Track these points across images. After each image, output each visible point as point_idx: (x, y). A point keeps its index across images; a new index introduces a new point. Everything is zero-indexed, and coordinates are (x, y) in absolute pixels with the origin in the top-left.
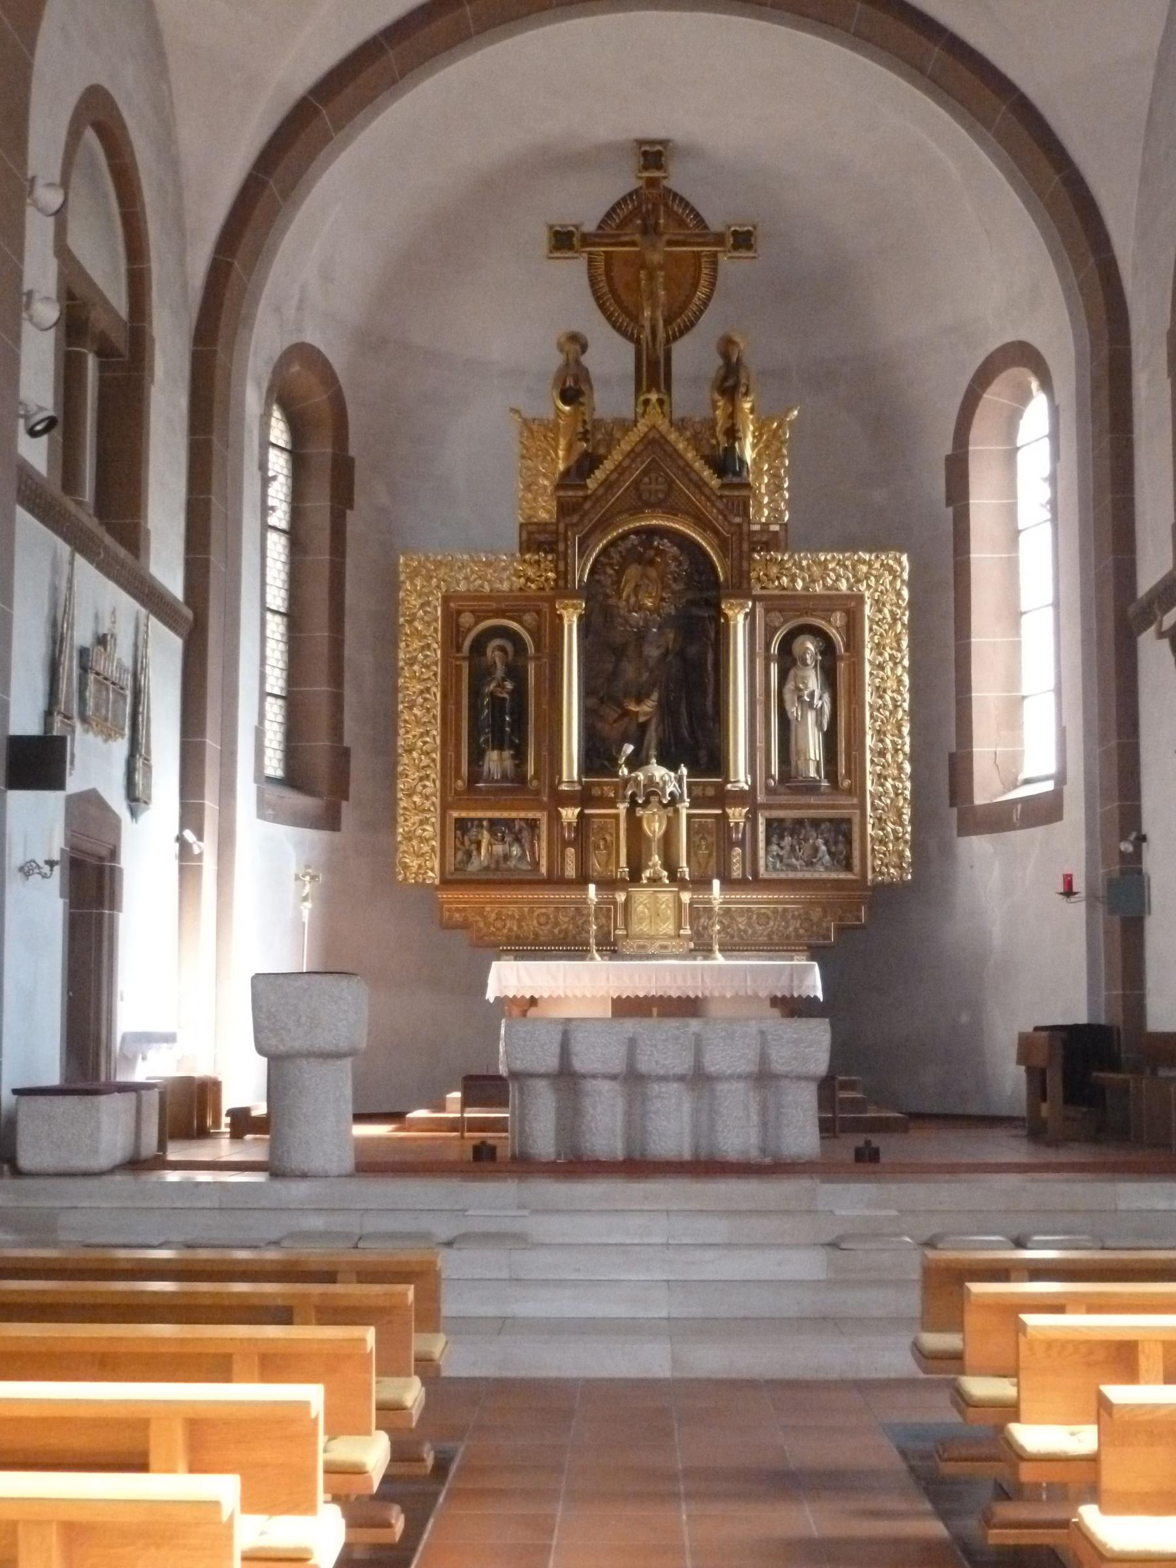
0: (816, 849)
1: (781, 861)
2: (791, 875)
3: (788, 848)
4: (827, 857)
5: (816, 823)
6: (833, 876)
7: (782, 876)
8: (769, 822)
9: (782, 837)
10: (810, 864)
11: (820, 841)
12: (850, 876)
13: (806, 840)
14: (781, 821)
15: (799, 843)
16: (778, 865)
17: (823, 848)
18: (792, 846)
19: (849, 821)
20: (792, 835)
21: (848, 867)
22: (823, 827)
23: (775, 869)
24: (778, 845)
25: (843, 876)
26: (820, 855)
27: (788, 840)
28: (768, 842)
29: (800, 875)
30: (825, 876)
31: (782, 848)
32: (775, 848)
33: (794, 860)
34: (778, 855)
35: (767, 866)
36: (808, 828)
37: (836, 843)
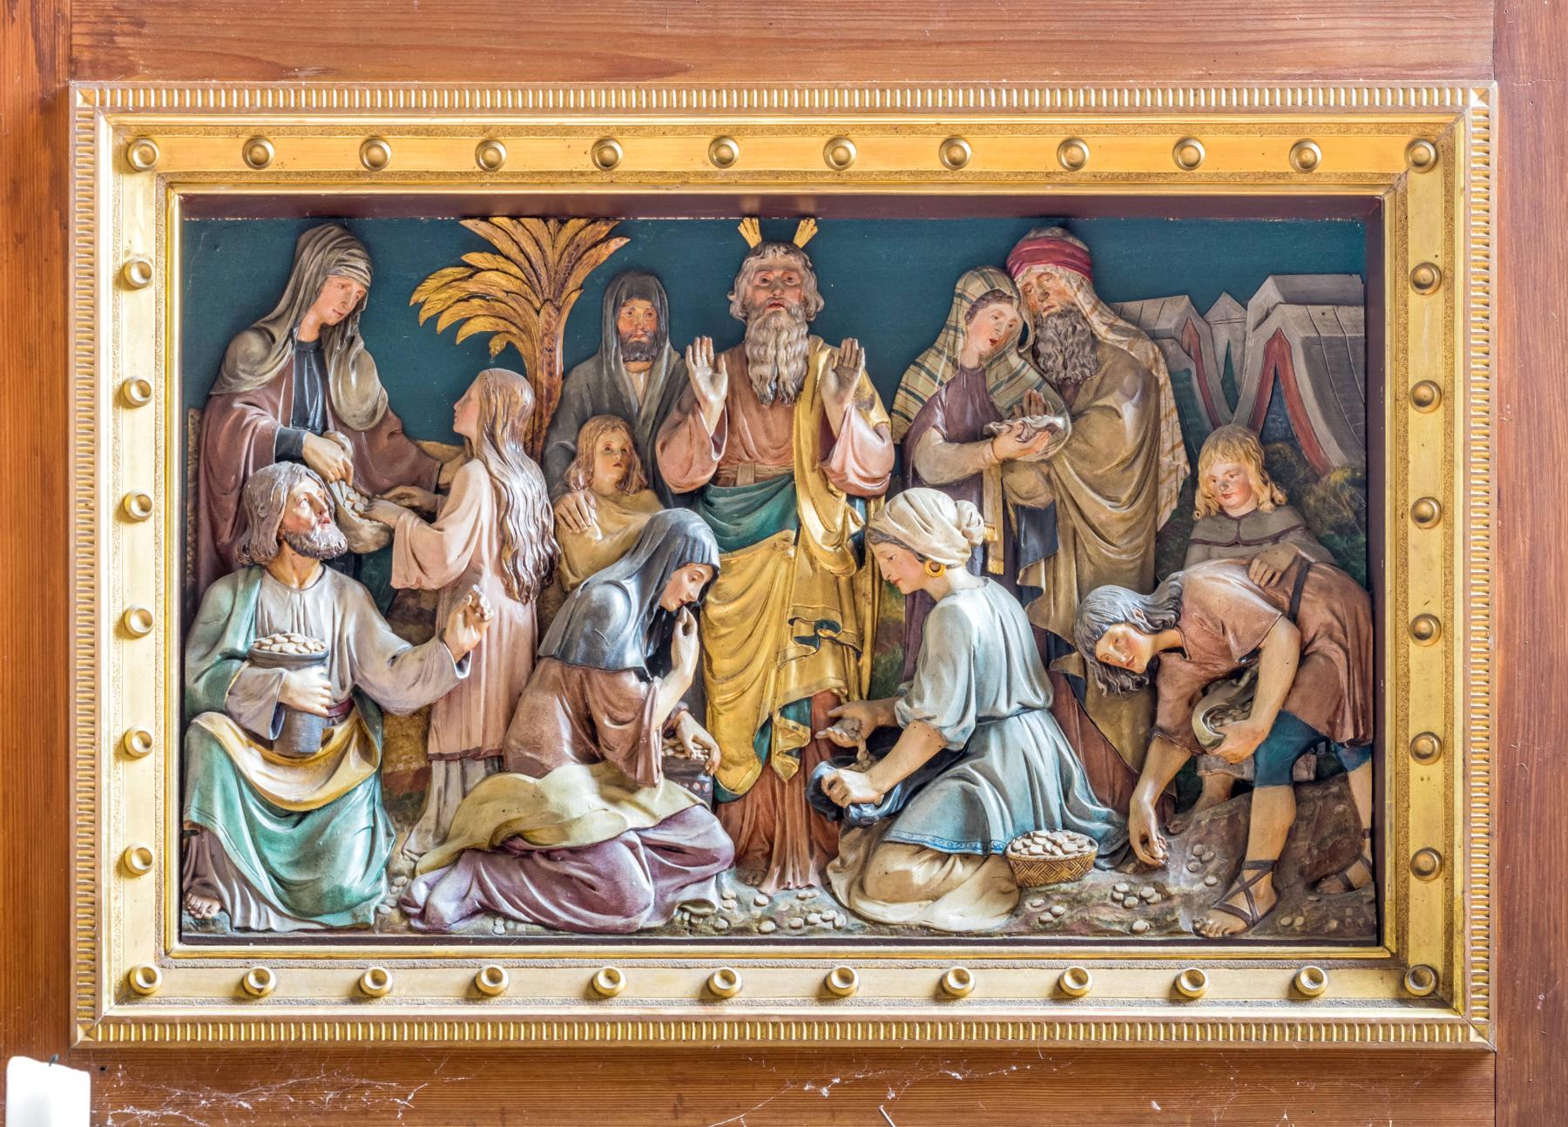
0: (893, 637)
1: (403, 800)
2: (539, 991)
3: (504, 613)
4: (1035, 742)
5: (889, 268)
6: (1123, 994)
7: (419, 994)
8: (241, 254)
9: (413, 459)
10: (803, 829)
11: (942, 528)
12: (1352, 1002)
13: (755, 505)
14: (404, 233)
15: (656, 557)
16: (353, 870)
17: (984, 616)
18: (551, 587)
19: (1343, 238)
20: (547, 445)
21: (1334, 887)
22: (980, 328)
23: (317, 915)
24: (360, 566)
25: (1242, 995)
26: (938, 707)
27: (492, 507)
28: (221, 541)
29: (653, 991)
30: (1008, 995)
31: (415, 615)
32: (315, 612)
33: (573, 790)
34: (357, 704)
35: (197, 861)
36: (785, 348)
37: (1162, 557)
